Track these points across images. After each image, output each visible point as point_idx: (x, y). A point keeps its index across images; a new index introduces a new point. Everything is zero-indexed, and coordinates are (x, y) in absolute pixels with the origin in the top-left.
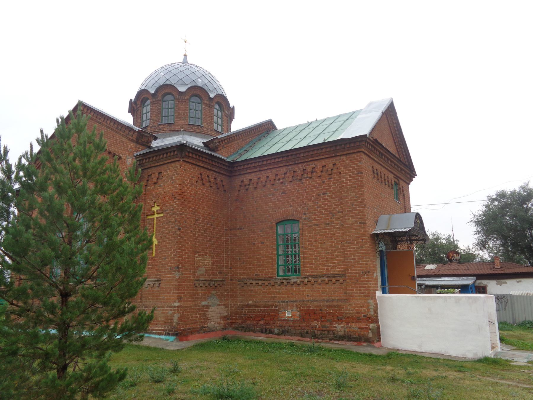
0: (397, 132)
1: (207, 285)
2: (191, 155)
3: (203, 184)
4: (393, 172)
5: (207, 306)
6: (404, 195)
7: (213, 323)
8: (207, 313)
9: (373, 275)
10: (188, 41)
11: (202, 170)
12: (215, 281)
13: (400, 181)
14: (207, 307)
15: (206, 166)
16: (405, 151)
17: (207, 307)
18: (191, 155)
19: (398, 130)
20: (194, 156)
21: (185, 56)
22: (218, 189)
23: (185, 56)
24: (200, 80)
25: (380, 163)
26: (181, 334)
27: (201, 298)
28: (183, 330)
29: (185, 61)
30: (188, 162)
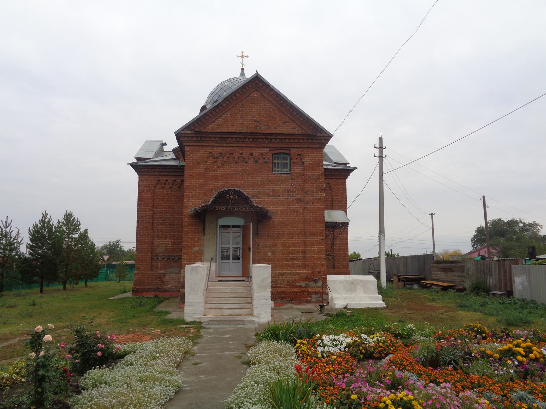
0: (281, 102)
1: (166, 259)
2: (143, 170)
3: (163, 187)
4: (265, 145)
5: (164, 273)
6: (303, 163)
7: (169, 286)
8: (164, 279)
9: (191, 249)
10: (245, 54)
11: (160, 178)
12: (174, 256)
13: (292, 150)
14: (164, 274)
15: (164, 174)
16: (301, 116)
17: (164, 274)
18: (143, 170)
19: (281, 100)
20: (147, 170)
21: (243, 69)
22: (179, 188)
23: (243, 69)
24: (225, 93)
25: (231, 145)
26: (136, 291)
27: (161, 268)
28: (138, 289)
29: (243, 74)
30: (144, 175)
